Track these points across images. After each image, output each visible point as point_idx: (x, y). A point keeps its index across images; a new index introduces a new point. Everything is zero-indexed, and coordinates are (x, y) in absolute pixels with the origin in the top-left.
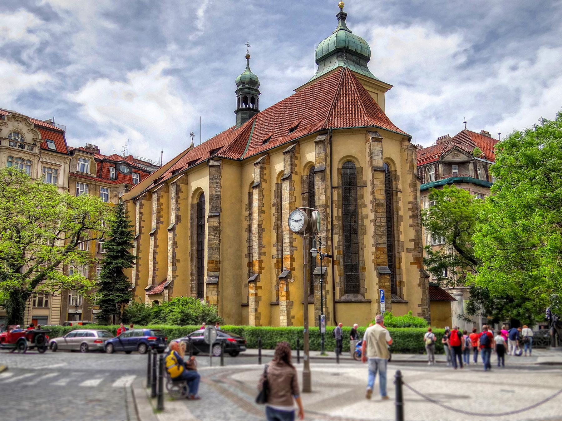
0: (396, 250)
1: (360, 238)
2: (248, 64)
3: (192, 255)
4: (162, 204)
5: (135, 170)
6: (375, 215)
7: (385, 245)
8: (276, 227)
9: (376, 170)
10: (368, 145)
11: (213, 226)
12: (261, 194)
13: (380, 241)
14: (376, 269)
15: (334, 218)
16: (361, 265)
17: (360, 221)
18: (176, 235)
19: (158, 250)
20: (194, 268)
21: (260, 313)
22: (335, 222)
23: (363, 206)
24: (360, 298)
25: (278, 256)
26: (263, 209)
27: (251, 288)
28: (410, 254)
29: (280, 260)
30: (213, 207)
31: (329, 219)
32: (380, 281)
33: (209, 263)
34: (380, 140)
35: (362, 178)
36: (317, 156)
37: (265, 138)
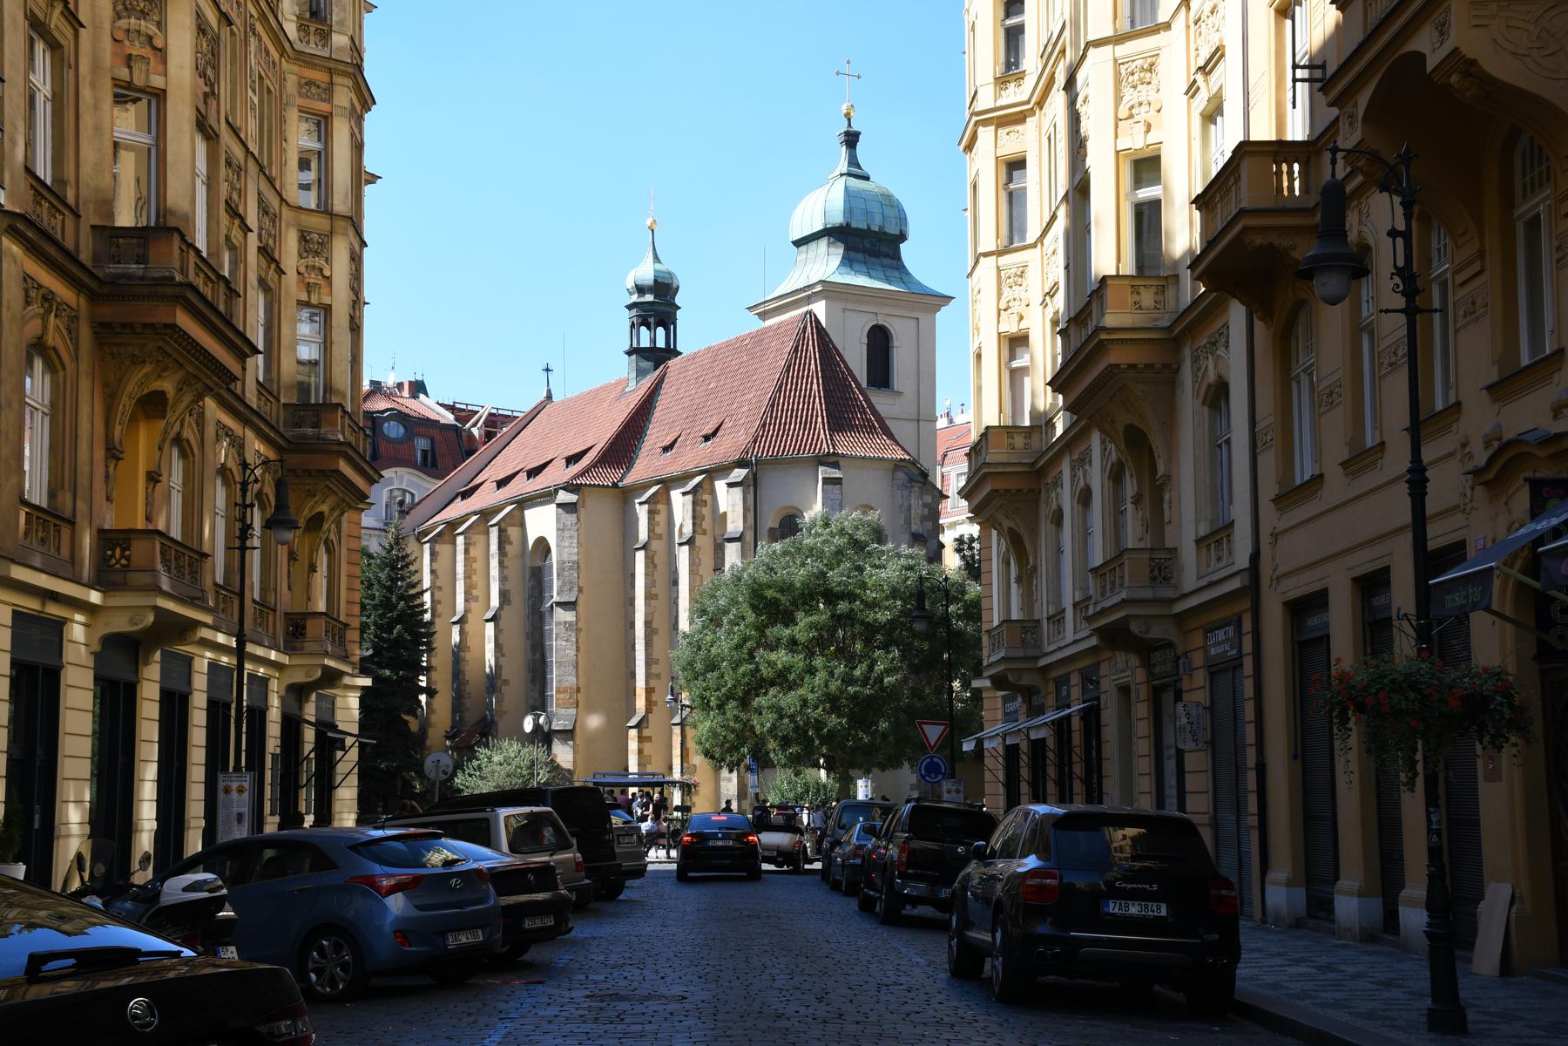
12: (650, 562)
26: (654, 591)
30: (564, 584)
37: (667, 443)
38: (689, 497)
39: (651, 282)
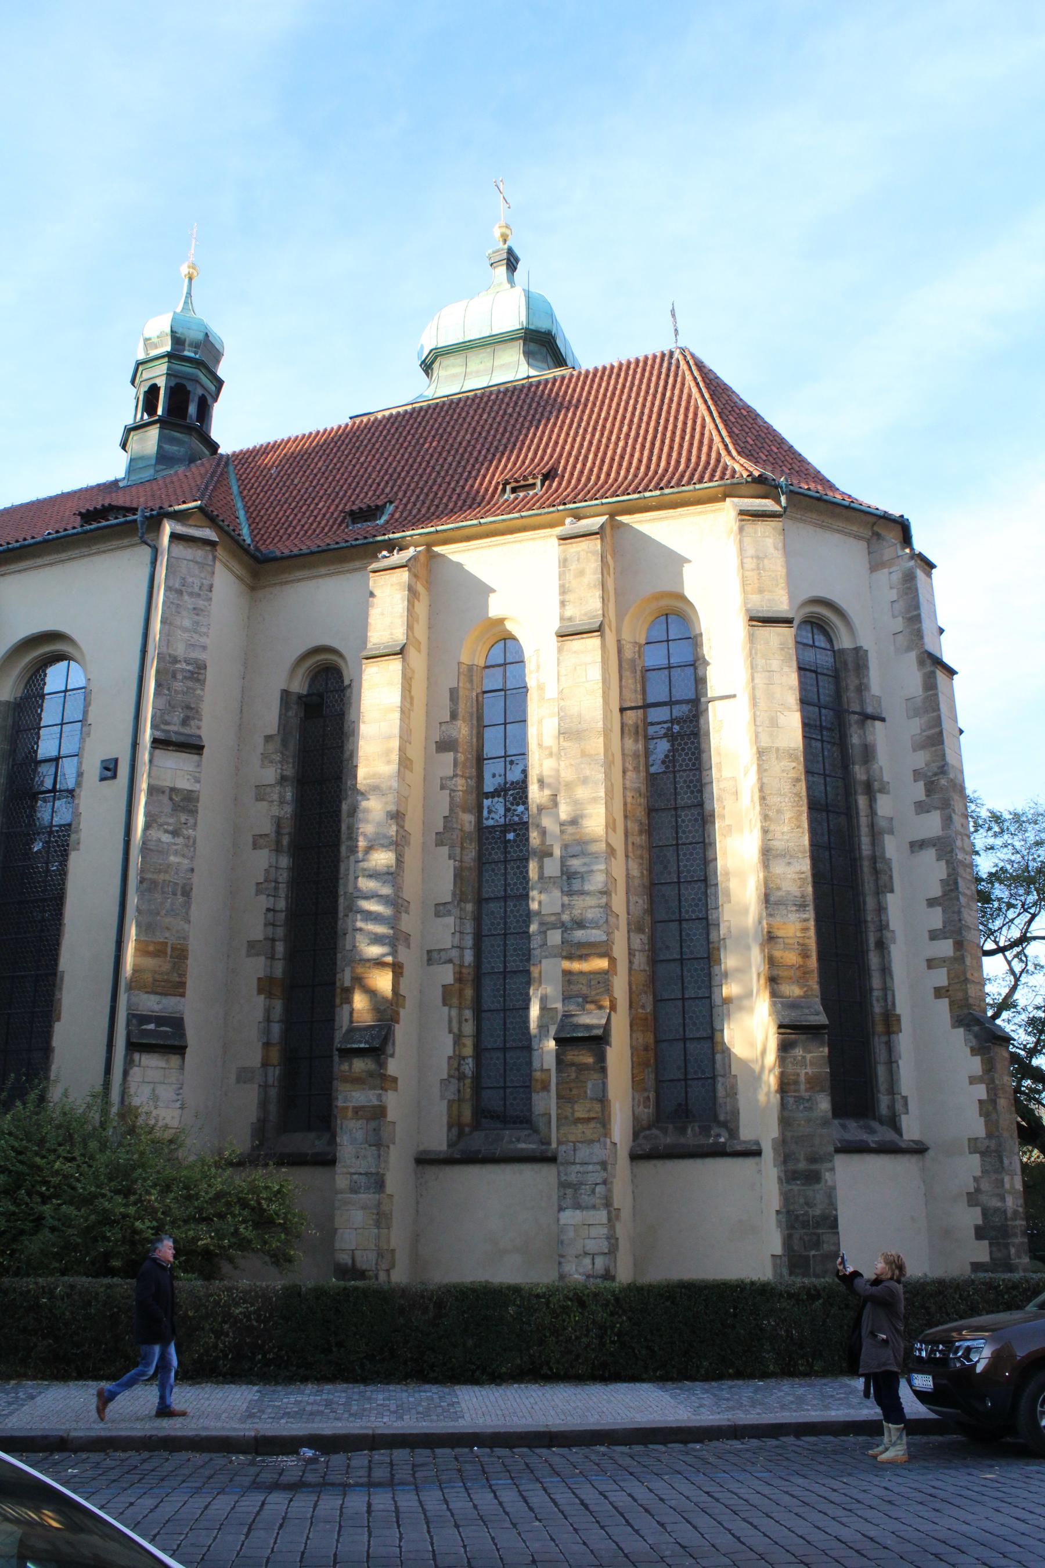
8: (456, 835)
11: (173, 790)
17: (865, 840)
21: (391, 1196)
23: (876, 785)
25: (462, 957)
27: (357, 1081)
30: (172, 706)
36: (750, 564)
39: (201, 337)
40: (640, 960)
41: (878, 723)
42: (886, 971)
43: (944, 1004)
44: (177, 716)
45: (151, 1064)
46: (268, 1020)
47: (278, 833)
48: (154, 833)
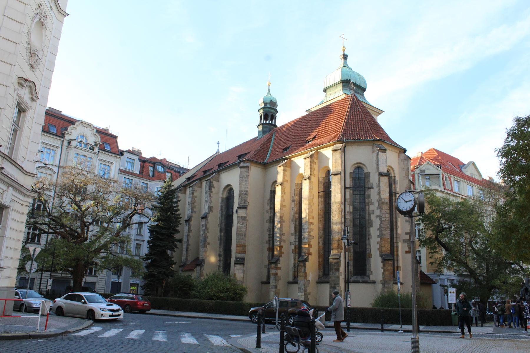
0: (395, 241)
1: (367, 230)
2: (269, 89)
3: (220, 239)
4: (196, 197)
5: (169, 170)
6: (381, 211)
7: (389, 237)
8: (294, 219)
9: (381, 174)
10: (374, 155)
13: (384, 232)
14: (381, 255)
15: (346, 213)
16: (367, 253)
17: (367, 216)
18: (208, 222)
19: (191, 234)
20: (221, 250)
21: (279, 290)
22: (347, 217)
24: (366, 279)
26: (284, 204)
27: (273, 268)
28: (406, 245)
29: (297, 246)
30: (242, 200)
31: (343, 214)
32: (384, 265)
33: (237, 246)
34: (384, 151)
35: (369, 181)
36: (334, 161)
37: (285, 147)
38: (309, 159)
39: (269, 101)
40: (321, 244)
41: (371, 189)
42: (370, 245)
43: (378, 252)
44: (243, 202)
45: (238, 266)
46: (269, 256)
47: (270, 219)
48: (239, 225)
